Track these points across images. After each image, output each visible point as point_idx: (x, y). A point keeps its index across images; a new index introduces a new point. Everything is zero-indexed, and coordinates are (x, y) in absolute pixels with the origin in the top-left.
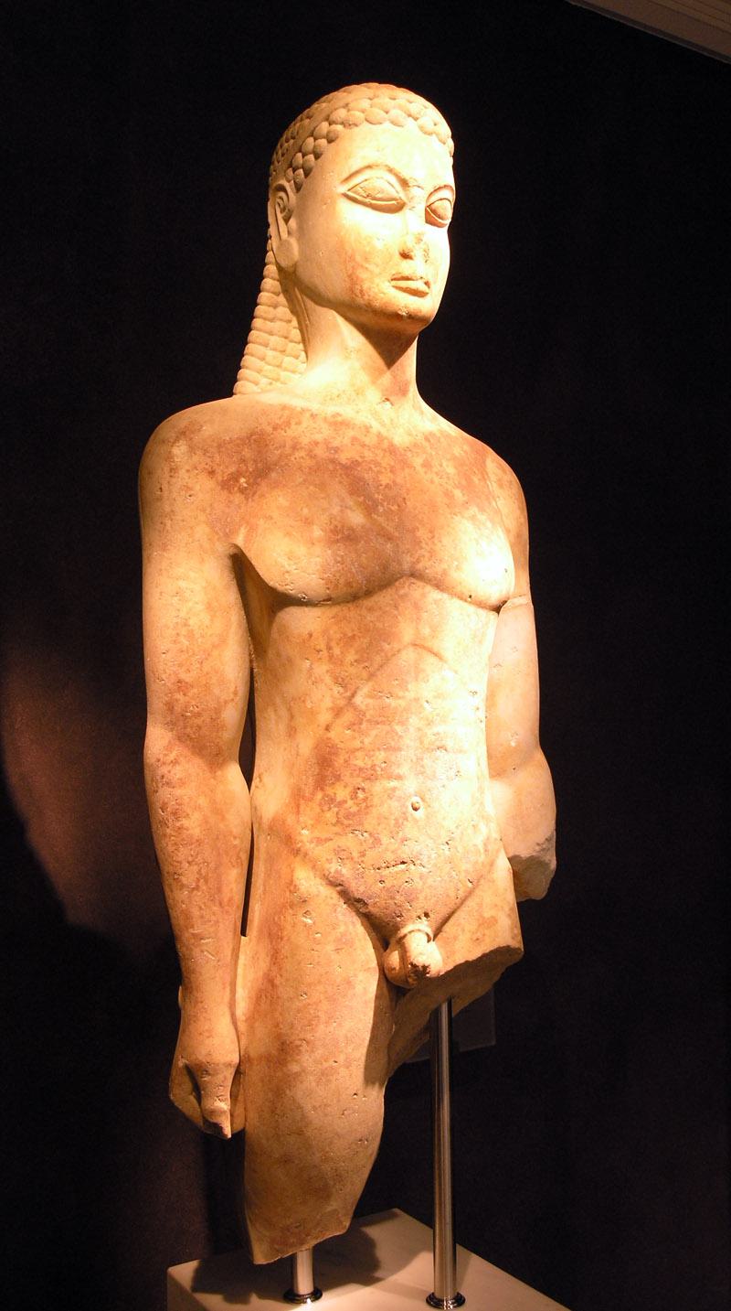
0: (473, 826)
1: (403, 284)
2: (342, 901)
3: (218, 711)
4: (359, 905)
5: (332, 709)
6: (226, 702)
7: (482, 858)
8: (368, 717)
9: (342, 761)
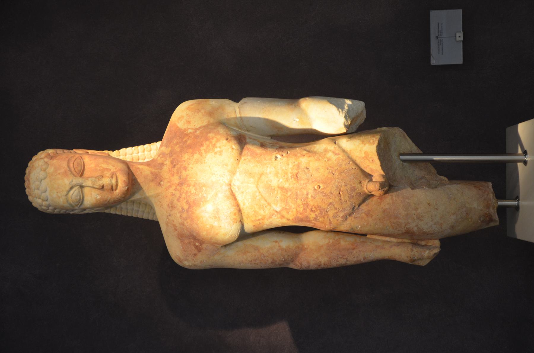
1: (114, 188)
2: (353, 215)
3: (282, 249)
6: (279, 246)
7: (341, 156)
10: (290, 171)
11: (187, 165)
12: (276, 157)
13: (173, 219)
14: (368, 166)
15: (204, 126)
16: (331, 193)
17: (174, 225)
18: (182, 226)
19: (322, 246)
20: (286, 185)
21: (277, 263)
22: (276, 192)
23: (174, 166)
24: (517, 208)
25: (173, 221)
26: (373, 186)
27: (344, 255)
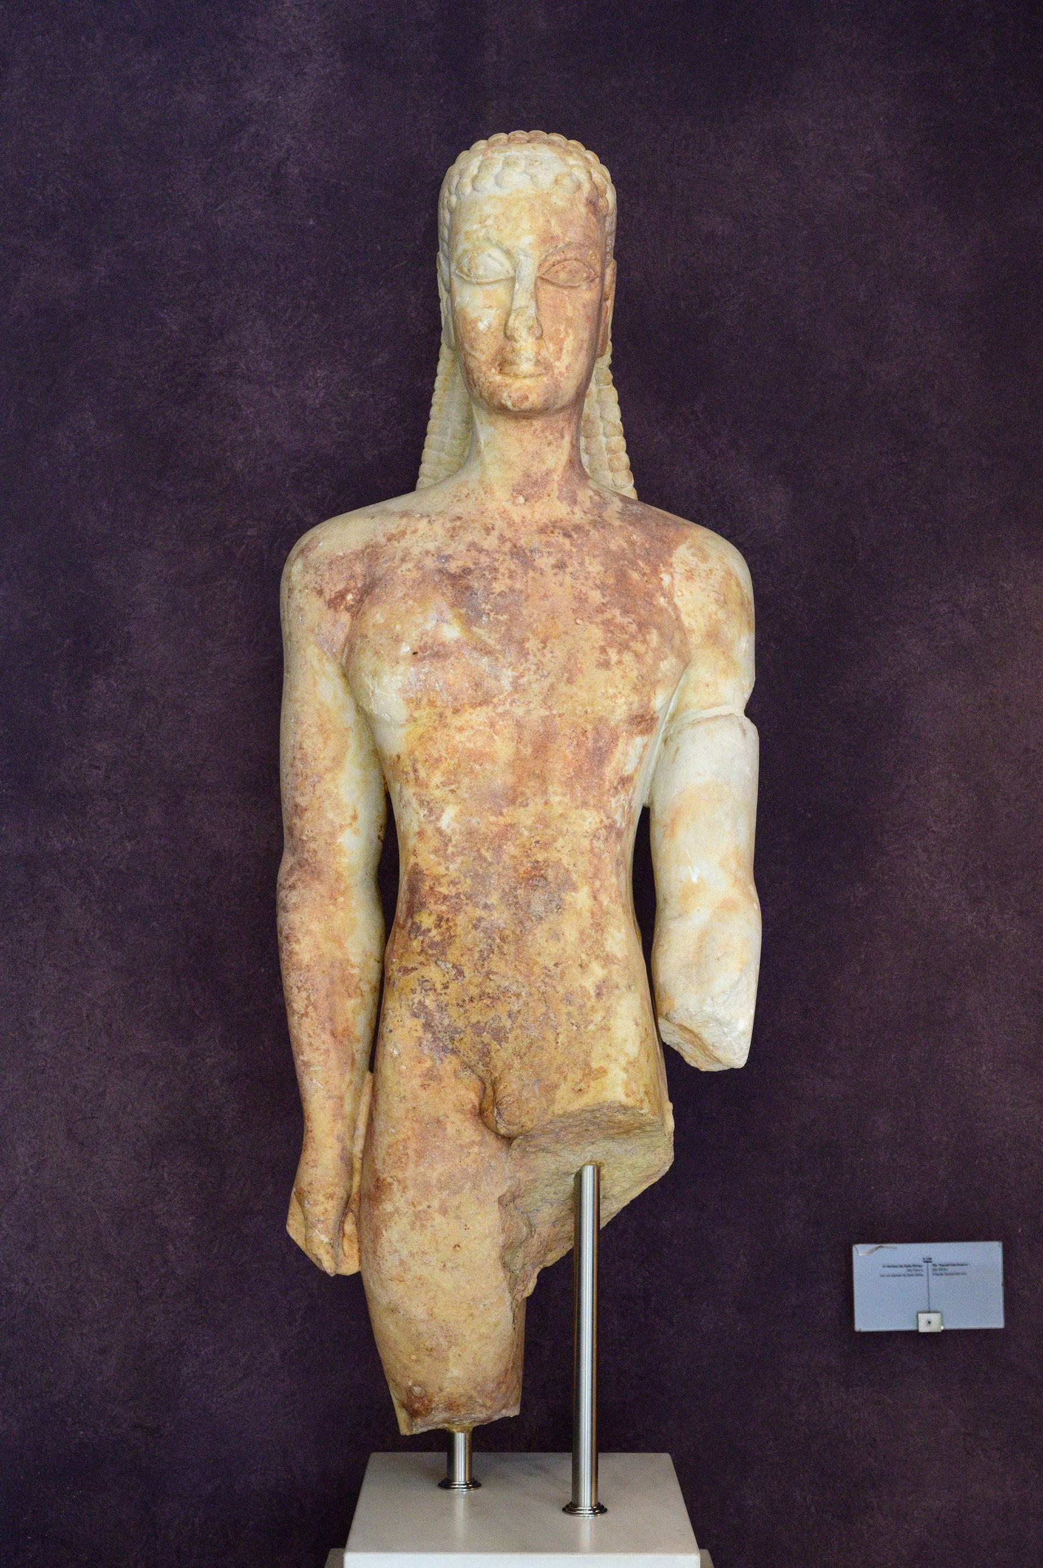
3: (333, 835)
6: (341, 827)
8: (454, 842)
9: (427, 888)
10: (554, 856)
11: (569, 569)
14: (565, 1078)
15: (678, 618)
16: (488, 974)
17: (403, 533)
18: (400, 554)
19: (341, 946)
20: (511, 849)
21: (296, 820)
23: (567, 535)
24: (447, 1483)
25: (415, 532)
27: (315, 1008)
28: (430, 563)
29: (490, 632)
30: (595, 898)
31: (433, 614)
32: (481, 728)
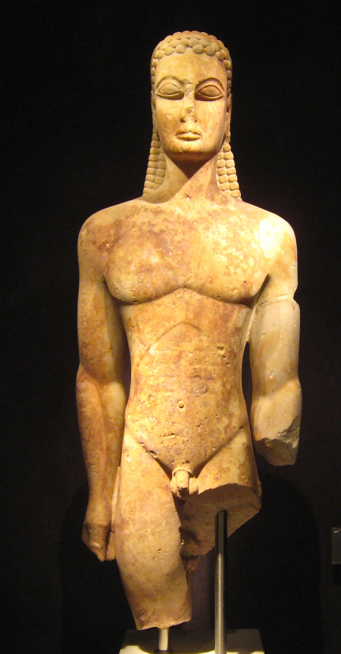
0: (217, 418)
3: (101, 357)
4: (153, 454)
5: (139, 355)
6: (105, 353)
7: (223, 436)
9: (143, 382)
11: (211, 230)
12: (222, 348)
13: (141, 214)
14: (210, 473)
15: (262, 253)
16: (173, 423)
17: (133, 215)
18: (131, 224)
21: (84, 350)
22: (174, 348)
23: (210, 215)
26: (182, 479)
28: (145, 228)
29: (173, 259)
30: (224, 386)
31: (146, 251)
32: (169, 305)
